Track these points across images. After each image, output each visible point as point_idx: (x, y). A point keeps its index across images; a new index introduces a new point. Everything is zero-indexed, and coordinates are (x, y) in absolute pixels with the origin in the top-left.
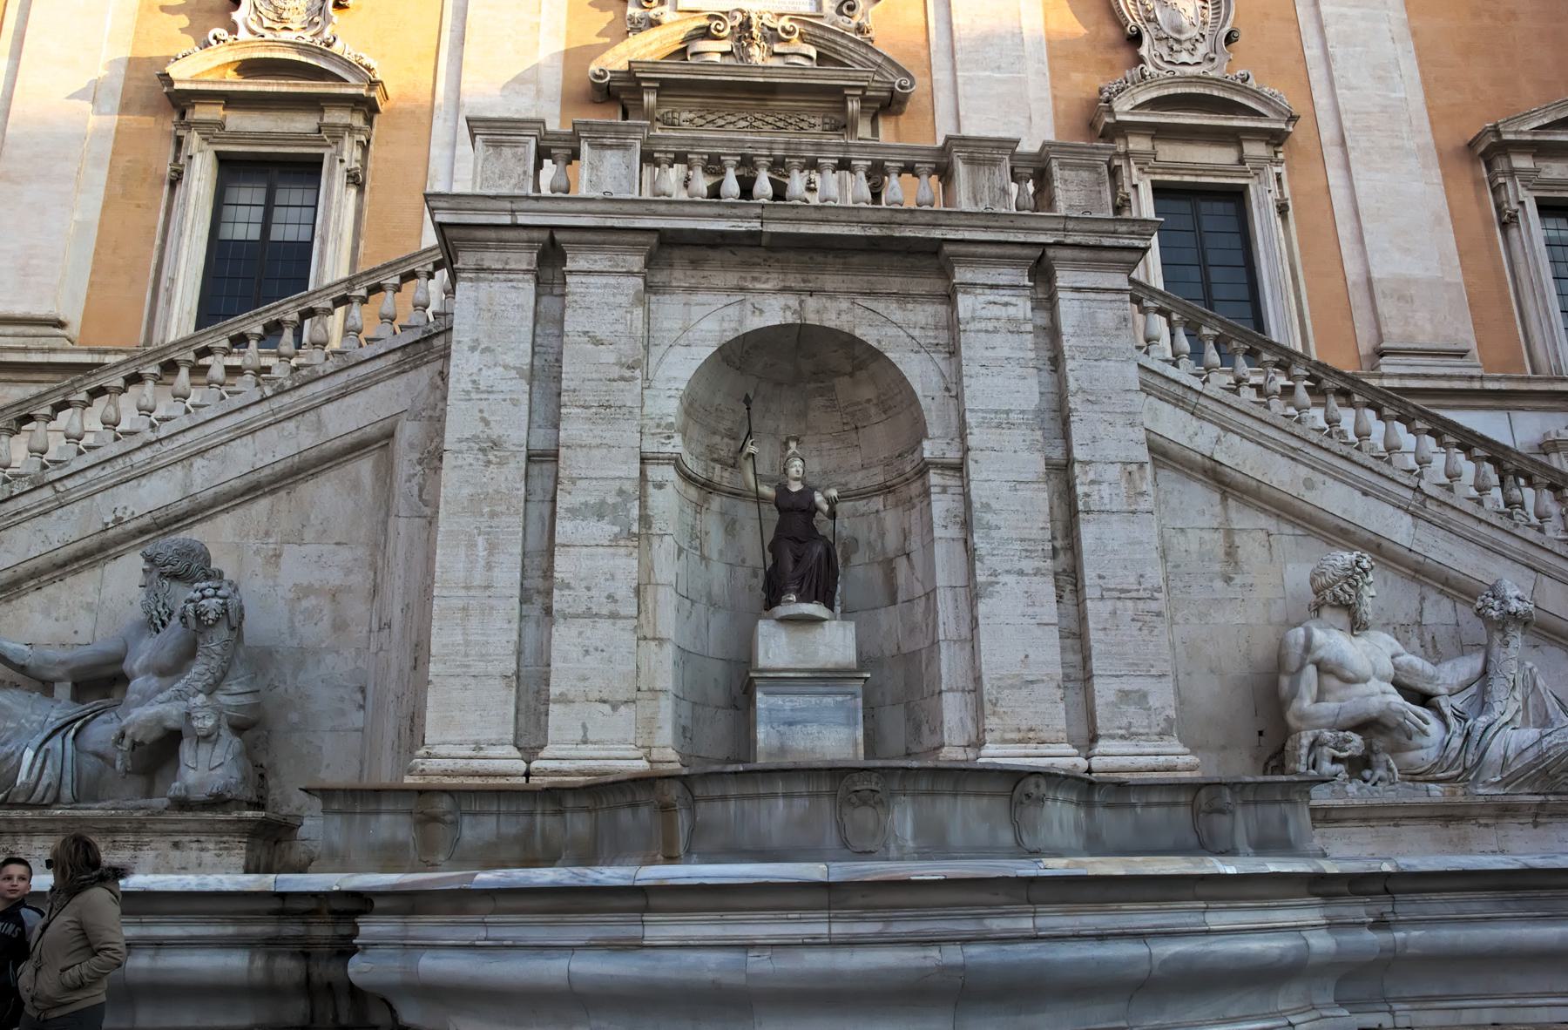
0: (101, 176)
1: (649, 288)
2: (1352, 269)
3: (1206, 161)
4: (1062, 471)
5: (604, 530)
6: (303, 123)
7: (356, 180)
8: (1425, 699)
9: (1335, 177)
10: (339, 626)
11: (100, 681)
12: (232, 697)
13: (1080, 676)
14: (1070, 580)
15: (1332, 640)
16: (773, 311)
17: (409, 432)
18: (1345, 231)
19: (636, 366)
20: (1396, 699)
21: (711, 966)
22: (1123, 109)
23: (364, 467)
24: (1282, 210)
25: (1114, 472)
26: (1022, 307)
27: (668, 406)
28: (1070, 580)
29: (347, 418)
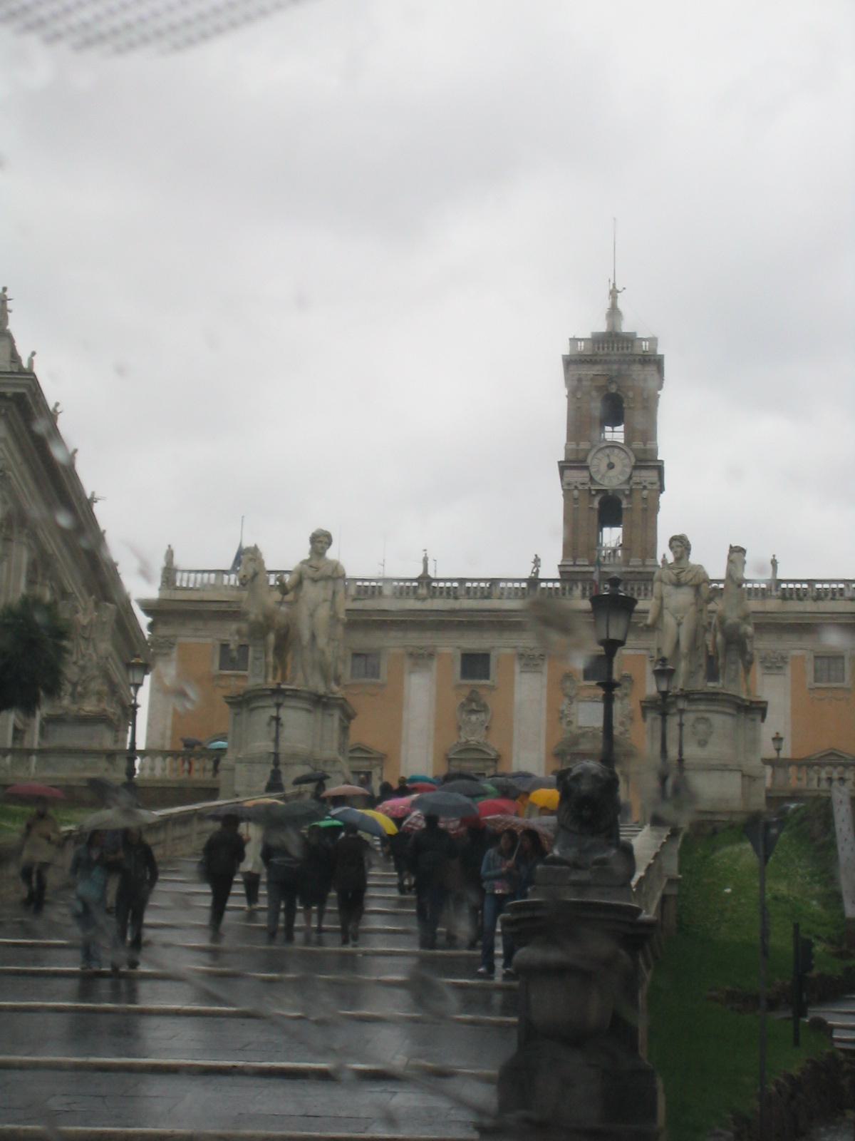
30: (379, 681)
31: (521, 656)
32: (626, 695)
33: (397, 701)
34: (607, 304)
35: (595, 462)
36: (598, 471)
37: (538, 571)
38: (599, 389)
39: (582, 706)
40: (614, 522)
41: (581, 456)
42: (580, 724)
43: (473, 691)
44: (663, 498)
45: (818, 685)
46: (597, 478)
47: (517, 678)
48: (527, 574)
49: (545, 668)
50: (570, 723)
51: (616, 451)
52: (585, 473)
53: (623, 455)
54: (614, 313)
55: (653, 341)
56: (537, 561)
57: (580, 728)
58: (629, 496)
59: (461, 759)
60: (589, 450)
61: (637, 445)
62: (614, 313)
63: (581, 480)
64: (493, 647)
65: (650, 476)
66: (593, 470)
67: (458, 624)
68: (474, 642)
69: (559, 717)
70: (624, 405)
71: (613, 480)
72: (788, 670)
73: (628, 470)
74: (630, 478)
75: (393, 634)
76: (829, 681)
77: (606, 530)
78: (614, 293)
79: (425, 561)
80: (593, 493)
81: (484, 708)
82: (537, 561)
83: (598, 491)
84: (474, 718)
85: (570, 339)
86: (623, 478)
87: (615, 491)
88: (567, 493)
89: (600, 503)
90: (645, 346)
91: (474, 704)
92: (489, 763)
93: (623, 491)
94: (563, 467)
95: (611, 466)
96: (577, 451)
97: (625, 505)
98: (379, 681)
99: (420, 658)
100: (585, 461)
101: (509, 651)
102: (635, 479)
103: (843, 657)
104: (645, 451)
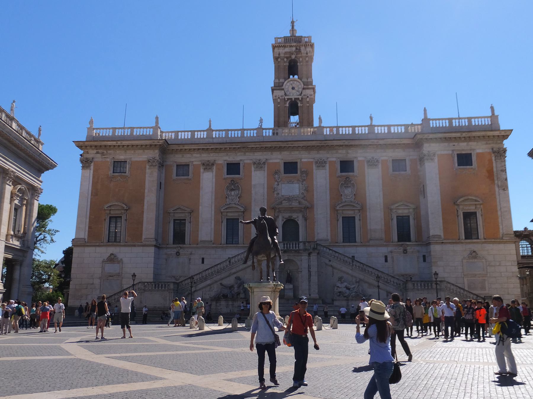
0: (213, 222)
2: (369, 227)
3: (350, 213)
6: (236, 214)
8: (349, 289)
9: (368, 213)
11: (231, 287)
13: (309, 289)
14: (309, 281)
15: (339, 285)
18: (368, 222)
20: (345, 289)
22: (338, 208)
24: (360, 220)
26: (307, 257)
28: (309, 281)
30: (189, 177)
31: (254, 163)
34: (290, 28)
35: (287, 87)
36: (288, 91)
37: (262, 125)
38: (287, 58)
39: (283, 185)
40: (294, 114)
41: (281, 84)
43: (232, 181)
44: (315, 105)
45: (394, 173)
46: (288, 93)
47: (253, 173)
48: (256, 126)
50: (278, 194)
51: (295, 82)
52: (283, 92)
53: (298, 84)
55: (309, 37)
56: (261, 121)
57: (283, 196)
58: (302, 101)
59: (227, 212)
60: (283, 83)
61: (305, 80)
65: (309, 92)
66: (286, 90)
67: (231, 154)
69: (272, 190)
70: (298, 64)
72: (380, 166)
73: (301, 90)
74: (302, 93)
75: (195, 155)
76: (399, 171)
77: (292, 117)
78: (293, 22)
79: (210, 121)
82: (261, 121)
83: (288, 99)
84: (233, 193)
86: (298, 93)
87: (295, 98)
88: (275, 101)
90: (306, 40)
91: (233, 186)
93: (299, 98)
94: (273, 90)
96: (279, 83)
97: (299, 105)
98: (189, 177)
99: (208, 166)
101: (248, 161)
103: (405, 160)
104: (307, 82)
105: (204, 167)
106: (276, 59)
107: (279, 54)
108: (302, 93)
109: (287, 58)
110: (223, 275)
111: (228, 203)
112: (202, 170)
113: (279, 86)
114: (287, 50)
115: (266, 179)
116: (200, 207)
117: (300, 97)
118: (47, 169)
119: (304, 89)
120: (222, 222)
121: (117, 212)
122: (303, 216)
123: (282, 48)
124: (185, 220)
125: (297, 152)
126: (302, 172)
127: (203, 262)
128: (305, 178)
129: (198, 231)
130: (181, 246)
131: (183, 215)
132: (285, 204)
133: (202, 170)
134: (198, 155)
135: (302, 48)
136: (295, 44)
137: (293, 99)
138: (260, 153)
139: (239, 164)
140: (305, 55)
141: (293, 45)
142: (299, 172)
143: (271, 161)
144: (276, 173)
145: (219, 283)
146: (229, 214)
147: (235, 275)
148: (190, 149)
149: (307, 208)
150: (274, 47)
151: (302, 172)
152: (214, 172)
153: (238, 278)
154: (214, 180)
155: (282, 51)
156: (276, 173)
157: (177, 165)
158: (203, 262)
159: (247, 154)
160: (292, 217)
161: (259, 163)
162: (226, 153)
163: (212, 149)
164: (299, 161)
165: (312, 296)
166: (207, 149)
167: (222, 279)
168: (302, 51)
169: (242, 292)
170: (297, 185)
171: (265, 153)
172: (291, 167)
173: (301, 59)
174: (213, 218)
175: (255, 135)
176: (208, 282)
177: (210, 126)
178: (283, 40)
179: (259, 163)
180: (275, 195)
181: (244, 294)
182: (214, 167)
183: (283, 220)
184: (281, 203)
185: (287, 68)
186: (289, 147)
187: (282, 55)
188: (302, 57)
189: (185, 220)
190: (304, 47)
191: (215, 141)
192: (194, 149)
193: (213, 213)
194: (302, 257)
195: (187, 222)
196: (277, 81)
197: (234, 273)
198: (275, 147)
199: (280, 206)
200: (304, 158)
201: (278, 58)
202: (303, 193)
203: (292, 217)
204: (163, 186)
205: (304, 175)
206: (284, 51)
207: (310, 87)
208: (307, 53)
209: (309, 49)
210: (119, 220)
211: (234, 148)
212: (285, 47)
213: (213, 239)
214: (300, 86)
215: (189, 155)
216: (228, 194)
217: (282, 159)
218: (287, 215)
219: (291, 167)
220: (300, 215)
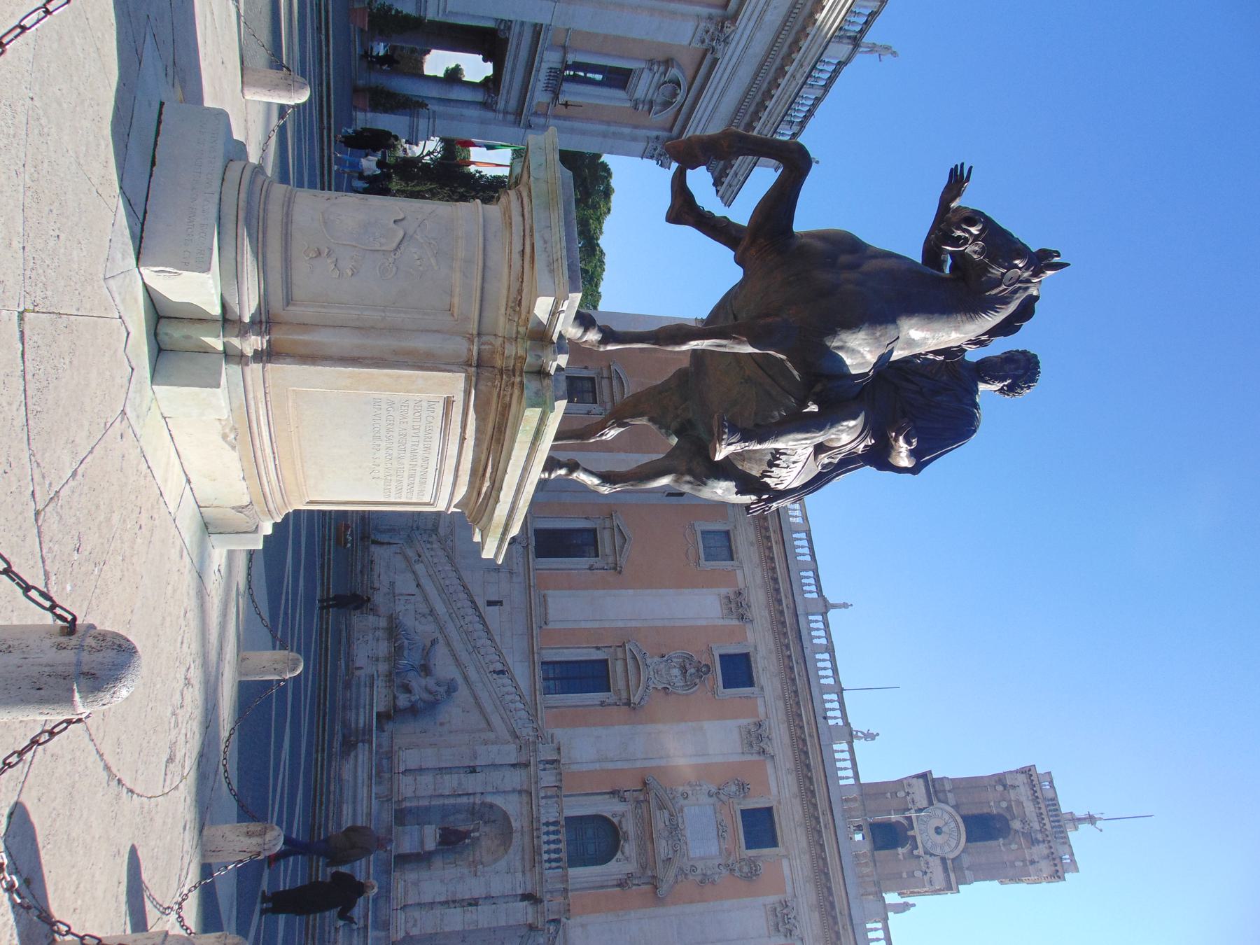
0: (596, 625)
1: (520, 792)
4: (474, 903)
5: (455, 784)
6: (621, 684)
7: (602, 704)
10: (442, 724)
11: (426, 669)
12: (420, 704)
14: (446, 903)
16: (515, 825)
17: (492, 736)
19: (497, 792)
21: (359, 797)
23: (483, 725)
25: (475, 917)
26: (520, 892)
27: (489, 799)
28: (446, 903)
29: (496, 720)
30: (702, 561)
32: (732, 870)
33: (683, 581)
35: (939, 812)
37: (859, 738)
38: (1009, 808)
41: (941, 795)
42: (685, 809)
43: (707, 666)
47: (732, 724)
49: (748, 758)
52: (924, 803)
54: (1076, 821)
56: (870, 736)
57: (681, 810)
60: (946, 802)
61: (966, 860)
62: (1076, 821)
63: (917, 798)
64: (762, 688)
68: (766, 667)
71: (923, 833)
73: (938, 852)
74: (931, 855)
75: (758, 573)
79: (845, 606)
80: (907, 814)
81: (690, 685)
82: (870, 736)
83: (909, 819)
84: (676, 672)
85: (1049, 773)
86: (929, 845)
87: (914, 838)
89: (898, 822)
91: (694, 671)
92: (624, 695)
94: (924, 776)
95: (938, 830)
97: (900, 850)
99: (737, 605)
100: (940, 801)
101: (761, 710)
102: (931, 859)
104: (961, 869)
105: (732, 596)
106: (1000, 779)
107: (1013, 787)
108: (931, 855)
109: (1009, 808)
110: (458, 646)
111: (649, 661)
112: (724, 591)
113: (935, 792)
114: (1029, 808)
115: (720, 759)
116: (631, 592)
117: (920, 851)
118: (717, 183)
119: (943, 860)
120: (598, 648)
121: (606, 391)
122: (630, 876)
123: (1030, 793)
124: (597, 556)
125: (804, 843)
126: (752, 862)
127: (490, 603)
128: (737, 873)
129: (570, 588)
130: (532, 548)
131: (608, 550)
132: (660, 820)
133: (724, 591)
134: (759, 580)
135: (1042, 849)
136: (1048, 827)
137: (910, 833)
138: (787, 740)
139: (751, 684)
140: (1028, 858)
141: (1046, 821)
142: (753, 853)
143: (770, 771)
144: (742, 787)
145: (437, 634)
146: (619, 666)
147: (460, 681)
148: (772, 559)
149: (654, 883)
150: (1028, 772)
151: (752, 862)
152: (721, 622)
153: (451, 688)
154: (704, 623)
155: (1023, 793)
156: (742, 787)
157: (727, 533)
158: (490, 603)
159: (781, 704)
160: (626, 840)
161: (760, 738)
162: (772, 647)
163: (782, 612)
164: (780, 850)
165: (401, 916)
166: (780, 602)
167: (448, 644)
168: (1035, 849)
169: (413, 699)
170: (714, 850)
171: (790, 753)
172: (760, 827)
173: (1014, 846)
174: (607, 625)
175: (831, 722)
176: (440, 608)
177: (835, 606)
178: (1051, 795)
179: (760, 738)
180: (681, 789)
181: (407, 704)
182: (735, 622)
183: (614, 815)
184: (662, 807)
185: (985, 810)
186: (817, 819)
187: (1012, 795)
188: (1020, 848)
189: (597, 556)
190: (1046, 852)
191: (802, 620)
192: (774, 569)
193: (620, 624)
194: (519, 875)
195: (592, 560)
196: (948, 787)
197: (466, 678)
198: (810, 779)
199: (653, 803)
200: (790, 860)
201: (1005, 786)
202: (694, 868)
203: (626, 840)
204: (674, 500)
205: (746, 869)
206: (1023, 799)
207: (952, 876)
208: (1032, 862)
209: (1045, 866)
210: (589, 396)
211: (792, 668)
212: (1035, 799)
213: (551, 626)
214: (947, 849)
215: (756, 558)
216: (670, 659)
217: (779, 802)
218: (629, 826)
219: (760, 827)
220: (631, 867)
